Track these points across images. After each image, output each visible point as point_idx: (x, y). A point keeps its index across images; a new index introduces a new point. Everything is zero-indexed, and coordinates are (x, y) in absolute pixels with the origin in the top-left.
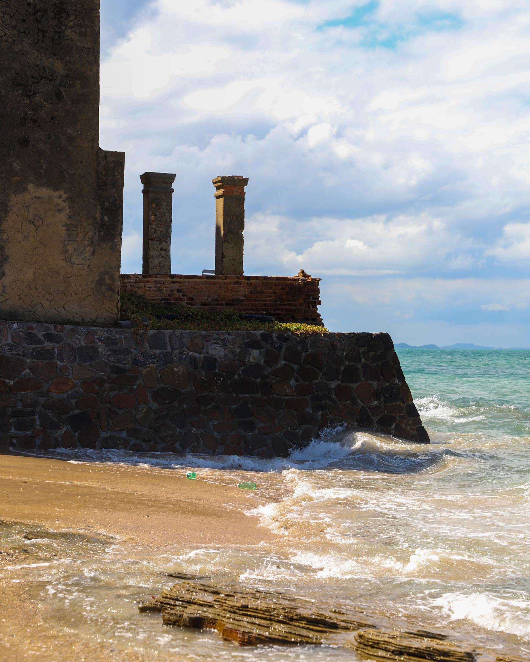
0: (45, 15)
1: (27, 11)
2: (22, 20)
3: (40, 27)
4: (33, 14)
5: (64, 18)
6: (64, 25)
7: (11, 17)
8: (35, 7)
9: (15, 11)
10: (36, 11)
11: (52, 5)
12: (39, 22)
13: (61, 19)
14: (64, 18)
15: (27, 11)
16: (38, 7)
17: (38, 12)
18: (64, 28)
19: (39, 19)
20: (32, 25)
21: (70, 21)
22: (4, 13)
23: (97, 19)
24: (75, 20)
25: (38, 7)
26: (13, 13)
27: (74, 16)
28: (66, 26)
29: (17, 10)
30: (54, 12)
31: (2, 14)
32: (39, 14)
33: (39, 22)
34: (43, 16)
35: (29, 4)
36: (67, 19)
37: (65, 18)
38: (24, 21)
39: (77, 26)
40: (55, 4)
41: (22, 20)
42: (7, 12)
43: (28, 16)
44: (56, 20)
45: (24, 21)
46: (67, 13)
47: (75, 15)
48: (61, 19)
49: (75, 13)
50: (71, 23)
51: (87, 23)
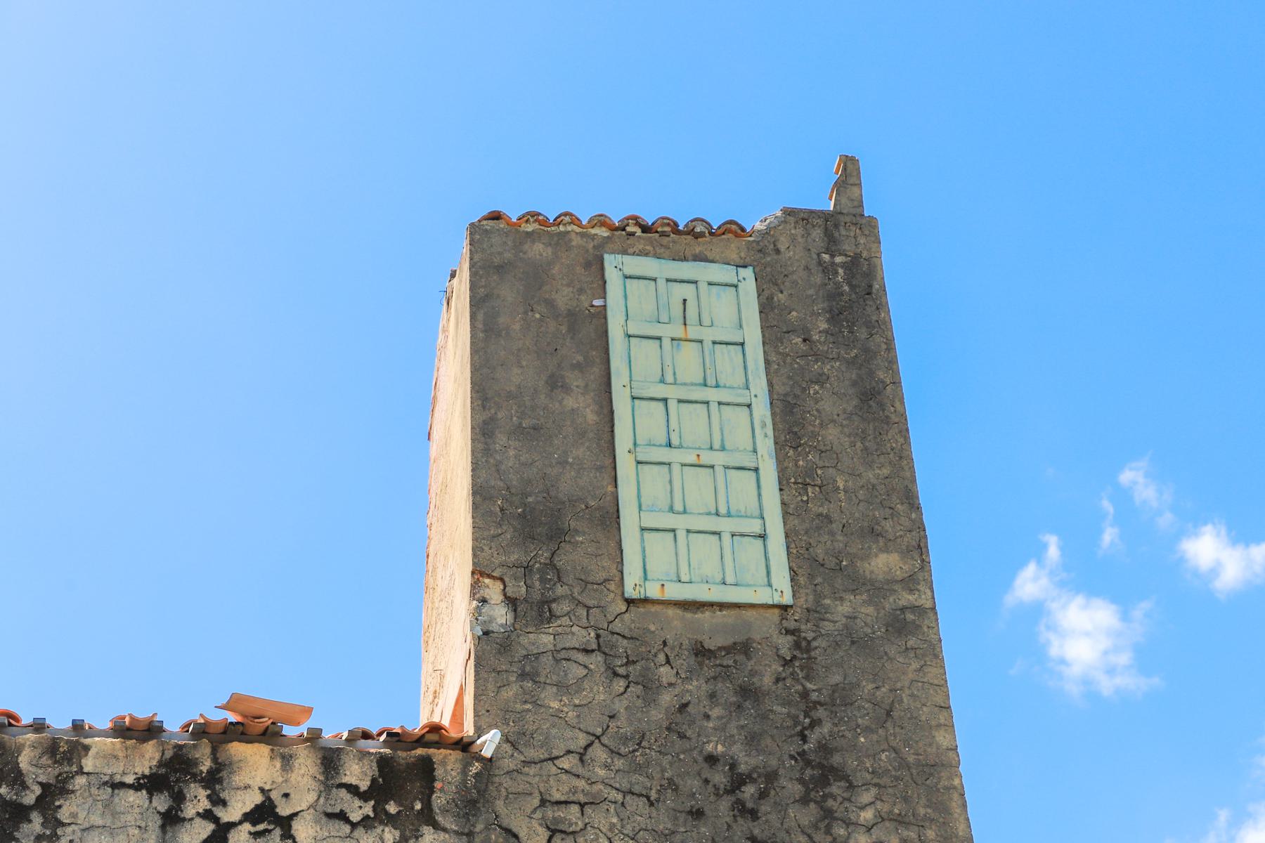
0: (773, 792)
1: (707, 781)
2: (690, 813)
3: (756, 832)
4: (727, 792)
5: (840, 799)
6: (844, 822)
7: (652, 804)
8: (733, 766)
9: (665, 782)
10: (738, 782)
11: (792, 757)
12: (753, 814)
13: (830, 803)
14: (840, 799)
15: (707, 781)
16: (743, 768)
17: (745, 783)
18: (842, 832)
19: (750, 805)
20: (729, 827)
21: (863, 808)
22: (625, 793)
23: (956, 796)
24: (879, 805)
25: (743, 768)
26: (659, 791)
27: (874, 791)
28: (848, 823)
29: (670, 780)
30: (801, 781)
31: (620, 797)
32: (749, 791)
33: (753, 814)
34: (763, 795)
35: (712, 759)
36: (849, 800)
37: (844, 799)
38: (697, 814)
39: (887, 824)
40: (802, 754)
41: (690, 813)
42: (637, 789)
43: (712, 798)
44: (812, 805)
45: (697, 814)
46: (848, 781)
47: (876, 785)
48: (830, 803)
49: (876, 780)
50: (867, 815)
51: (922, 811)
